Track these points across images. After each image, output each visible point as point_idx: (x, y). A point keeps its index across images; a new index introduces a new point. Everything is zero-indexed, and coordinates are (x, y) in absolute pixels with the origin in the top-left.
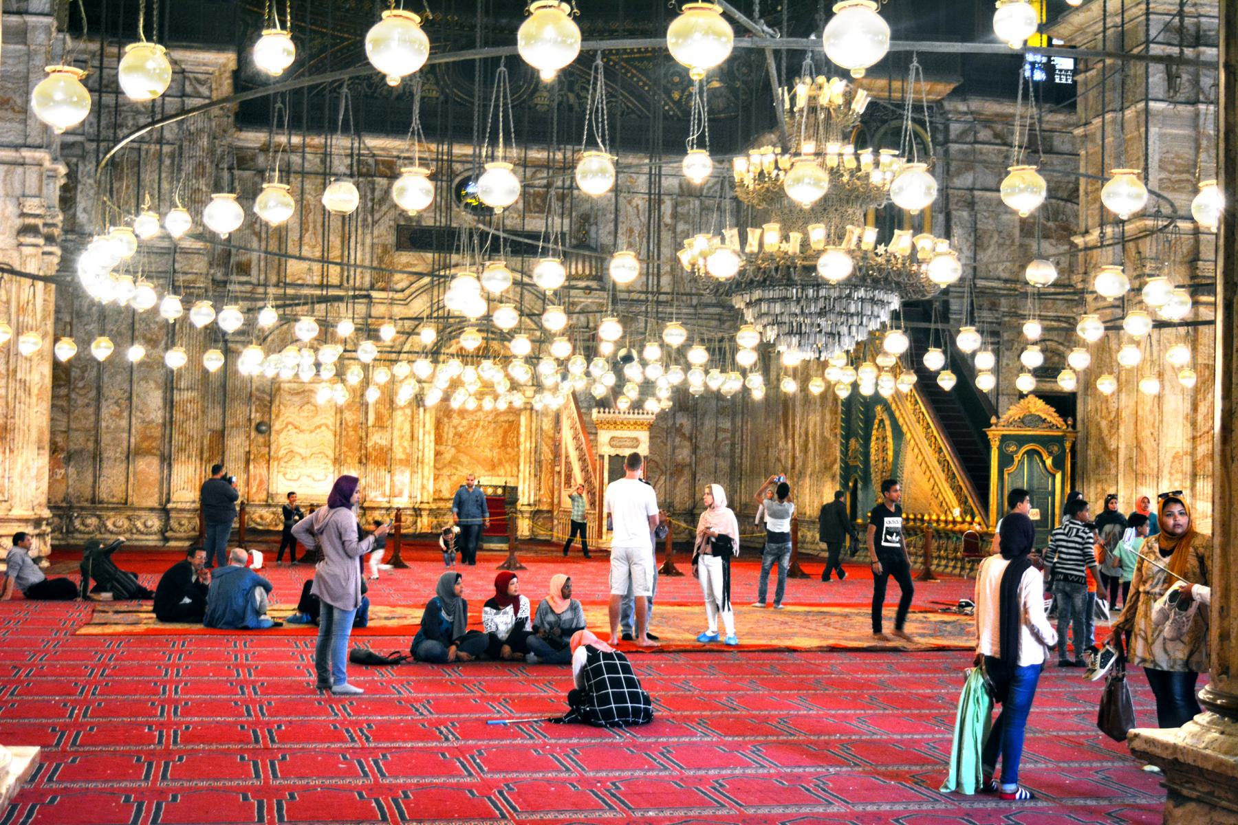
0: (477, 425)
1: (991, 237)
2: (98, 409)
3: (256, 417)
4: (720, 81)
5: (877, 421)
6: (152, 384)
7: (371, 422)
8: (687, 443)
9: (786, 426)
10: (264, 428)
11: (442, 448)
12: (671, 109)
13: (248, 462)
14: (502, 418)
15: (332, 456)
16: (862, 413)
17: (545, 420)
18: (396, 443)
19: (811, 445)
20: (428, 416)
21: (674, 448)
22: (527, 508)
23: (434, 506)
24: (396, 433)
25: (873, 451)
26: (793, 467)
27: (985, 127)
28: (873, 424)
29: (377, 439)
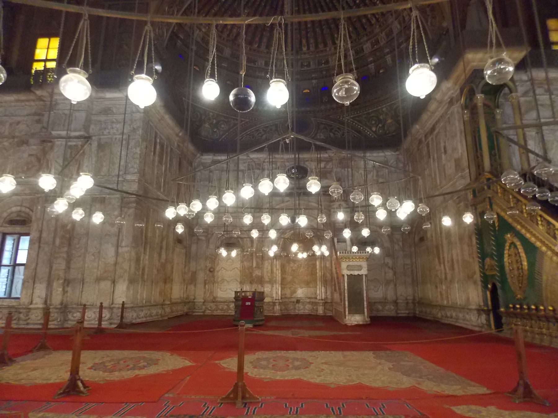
0: (301, 266)
1: (553, 143)
2: (85, 257)
3: (209, 265)
4: (392, 119)
5: (507, 245)
6: (110, 245)
7: (254, 265)
8: (391, 271)
9: (439, 259)
10: (212, 270)
11: (286, 276)
12: (372, 135)
13: (205, 284)
14: (310, 263)
15: (239, 280)
16: (494, 241)
17: (328, 263)
18: (265, 274)
19: (456, 266)
20: (278, 262)
21: (385, 273)
22: (321, 301)
23: (281, 301)
24: (265, 270)
25: (506, 264)
26: (446, 278)
27: (539, 87)
28: (504, 246)
29: (257, 273)
